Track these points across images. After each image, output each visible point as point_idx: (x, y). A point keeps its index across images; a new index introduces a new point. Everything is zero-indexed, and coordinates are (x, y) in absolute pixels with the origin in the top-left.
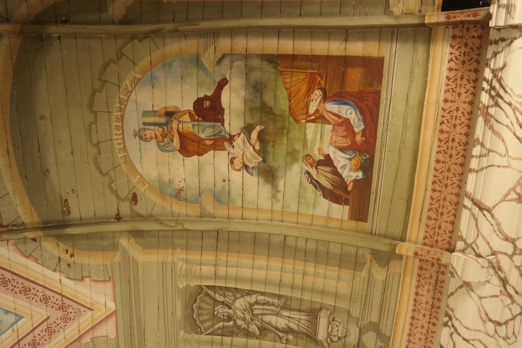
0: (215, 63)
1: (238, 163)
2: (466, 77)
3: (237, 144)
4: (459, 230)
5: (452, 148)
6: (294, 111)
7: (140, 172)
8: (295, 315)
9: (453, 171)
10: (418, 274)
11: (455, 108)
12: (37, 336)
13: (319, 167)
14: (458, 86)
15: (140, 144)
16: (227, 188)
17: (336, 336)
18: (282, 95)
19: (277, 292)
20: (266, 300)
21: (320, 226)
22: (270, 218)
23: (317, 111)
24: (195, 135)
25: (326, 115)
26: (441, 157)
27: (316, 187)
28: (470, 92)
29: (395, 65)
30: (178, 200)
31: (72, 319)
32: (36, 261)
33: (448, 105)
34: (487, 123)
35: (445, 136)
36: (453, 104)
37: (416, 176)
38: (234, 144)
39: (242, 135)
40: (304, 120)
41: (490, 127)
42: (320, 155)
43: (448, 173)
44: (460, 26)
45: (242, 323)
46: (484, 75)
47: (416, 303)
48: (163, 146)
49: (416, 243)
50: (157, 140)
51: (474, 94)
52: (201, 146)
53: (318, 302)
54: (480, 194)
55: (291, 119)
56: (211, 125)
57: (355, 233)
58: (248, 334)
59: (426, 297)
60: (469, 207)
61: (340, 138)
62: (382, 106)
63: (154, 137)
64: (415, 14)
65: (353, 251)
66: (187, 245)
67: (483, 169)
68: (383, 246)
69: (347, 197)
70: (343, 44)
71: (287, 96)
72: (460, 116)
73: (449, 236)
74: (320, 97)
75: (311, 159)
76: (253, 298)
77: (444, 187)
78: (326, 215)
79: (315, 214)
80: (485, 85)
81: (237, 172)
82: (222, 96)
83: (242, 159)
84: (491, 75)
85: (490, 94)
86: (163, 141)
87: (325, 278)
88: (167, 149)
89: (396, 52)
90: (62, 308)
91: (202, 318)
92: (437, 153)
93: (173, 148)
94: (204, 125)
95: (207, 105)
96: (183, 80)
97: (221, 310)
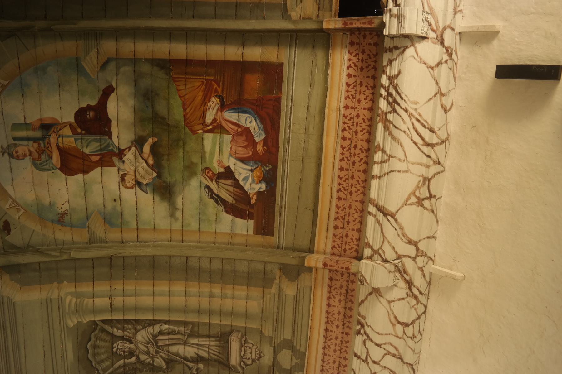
0: (99, 68)
1: (129, 180)
2: (364, 84)
3: (128, 159)
4: (366, 237)
5: (355, 155)
6: (190, 121)
7: (12, 196)
8: (204, 342)
9: (356, 178)
10: (328, 285)
11: (356, 114)
13: (219, 180)
14: (358, 92)
15: (10, 163)
16: (119, 209)
17: (249, 358)
18: (176, 104)
20: (171, 329)
21: (224, 244)
22: (169, 239)
23: (215, 120)
24: (78, 150)
25: (224, 124)
26: (344, 164)
27: (217, 202)
28: (369, 98)
29: (295, 71)
30: (62, 226)
33: (349, 111)
34: (386, 129)
35: (347, 143)
36: (353, 110)
37: (321, 184)
38: (125, 159)
39: (133, 148)
40: (201, 130)
41: (389, 133)
42: (220, 168)
43: (352, 180)
44: (357, 33)
45: (146, 357)
46: (382, 82)
47: (328, 315)
48: (40, 165)
49: (324, 254)
50: (31, 158)
51: (373, 101)
52: (86, 162)
53: (228, 325)
54: (384, 199)
55: (187, 130)
56: (96, 139)
57: (262, 248)
59: (338, 307)
60: (374, 213)
61: (240, 149)
62: (283, 114)
63: (28, 154)
64: (313, 19)
65: (260, 267)
66: (75, 276)
67: (384, 175)
68: (291, 259)
69: (251, 210)
70: (239, 48)
71: (181, 105)
72: (360, 122)
73: (357, 244)
74: (218, 106)
75: (211, 172)
76: (156, 329)
77: (349, 195)
78: (229, 231)
79: (218, 231)
80: (383, 92)
81: (129, 190)
82: (108, 106)
83: (134, 175)
84: (388, 81)
85: (388, 101)
86: (39, 158)
87: (233, 298)
88: (45, 167)
89: (295, 57)
91: (98, 359)
92: (341, 160)
93: (52, 165)
94: (89, 139)
95: (91, 116)
96: (61, 88)
97: (120, 346)
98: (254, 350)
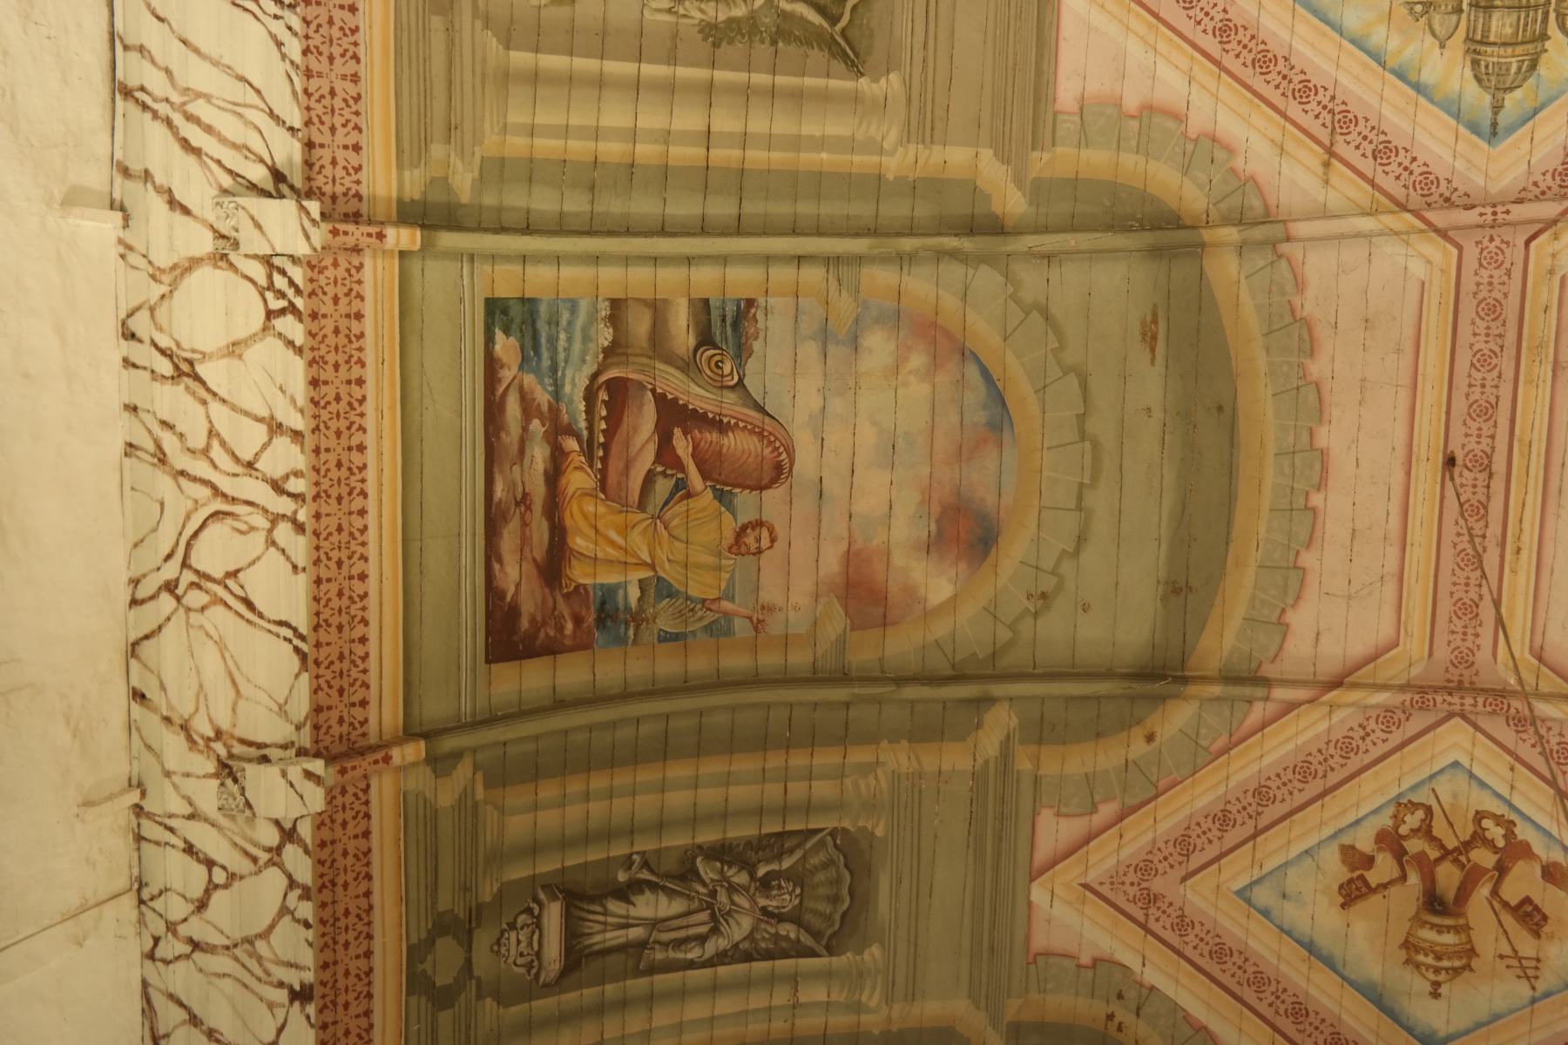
8: (614, 937)
12: (1215, 840)
17: (522, 928)
19: (657, 978)
31: (1132, 869)
32: (1187, 1017)
45: (735, 880)
58: (721, 853)
76: (711, 947)
90: (1151, 899)
91: (832, 873)
97: (784, 900)
98: (513, 952)
